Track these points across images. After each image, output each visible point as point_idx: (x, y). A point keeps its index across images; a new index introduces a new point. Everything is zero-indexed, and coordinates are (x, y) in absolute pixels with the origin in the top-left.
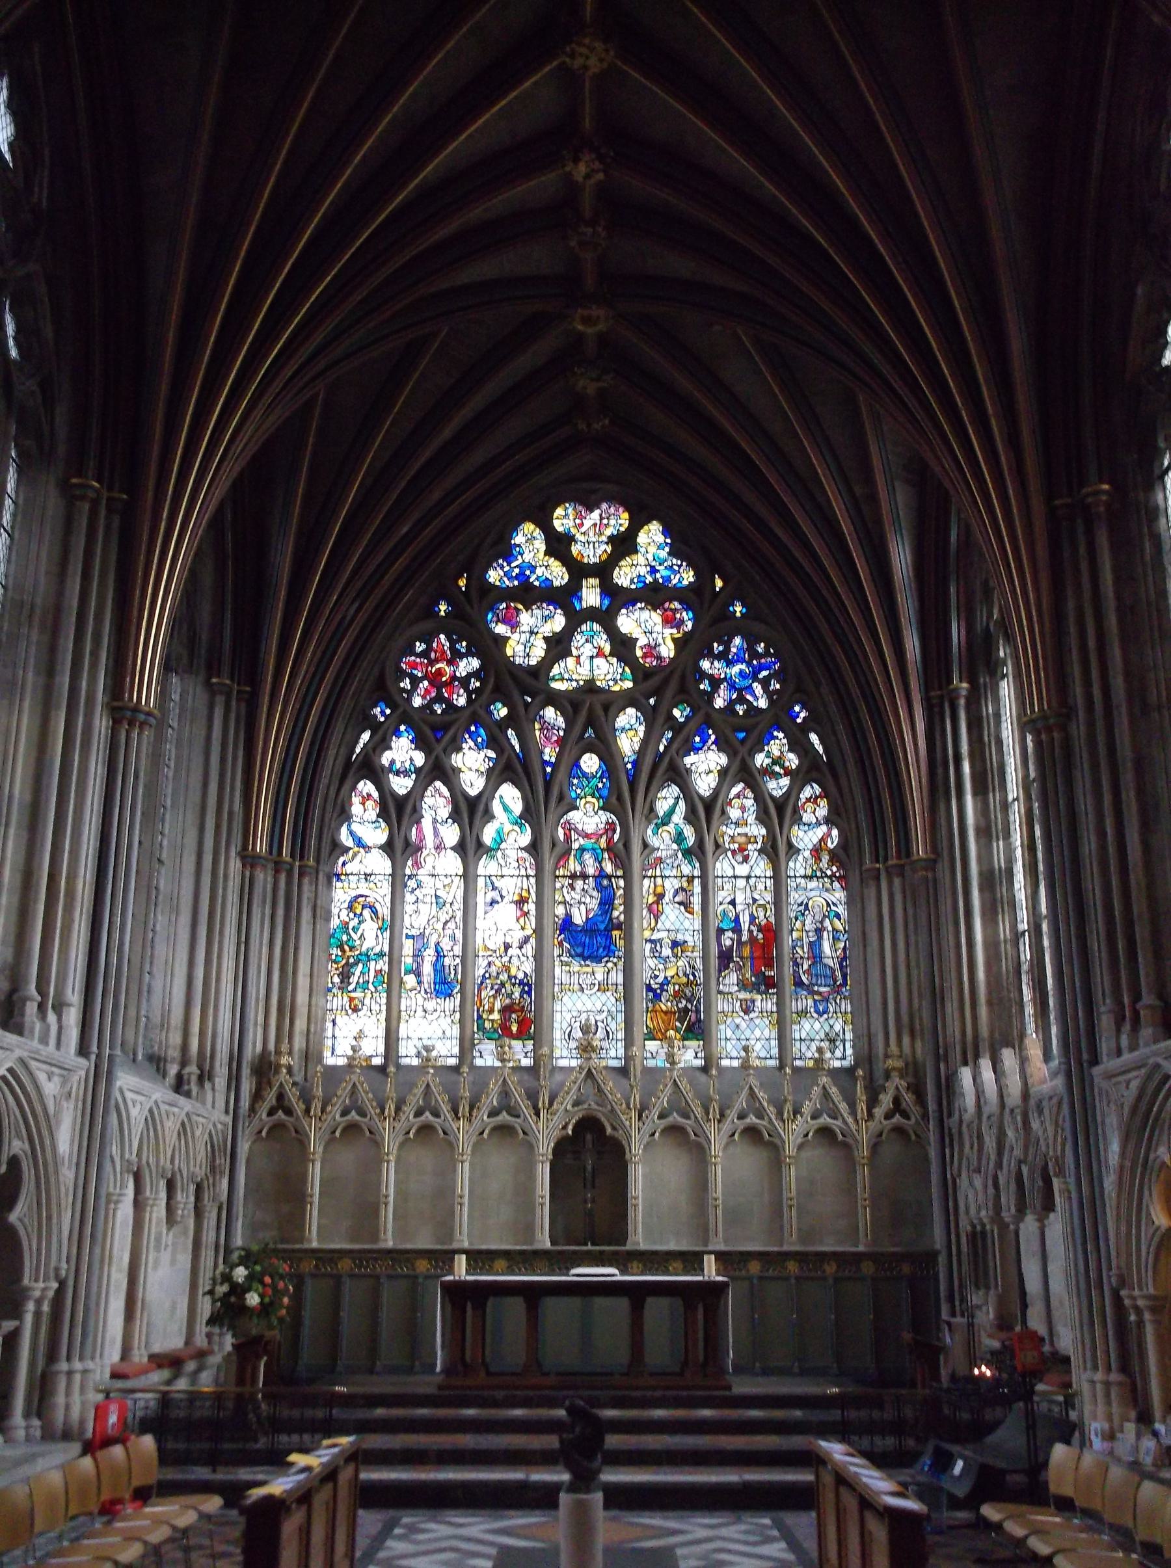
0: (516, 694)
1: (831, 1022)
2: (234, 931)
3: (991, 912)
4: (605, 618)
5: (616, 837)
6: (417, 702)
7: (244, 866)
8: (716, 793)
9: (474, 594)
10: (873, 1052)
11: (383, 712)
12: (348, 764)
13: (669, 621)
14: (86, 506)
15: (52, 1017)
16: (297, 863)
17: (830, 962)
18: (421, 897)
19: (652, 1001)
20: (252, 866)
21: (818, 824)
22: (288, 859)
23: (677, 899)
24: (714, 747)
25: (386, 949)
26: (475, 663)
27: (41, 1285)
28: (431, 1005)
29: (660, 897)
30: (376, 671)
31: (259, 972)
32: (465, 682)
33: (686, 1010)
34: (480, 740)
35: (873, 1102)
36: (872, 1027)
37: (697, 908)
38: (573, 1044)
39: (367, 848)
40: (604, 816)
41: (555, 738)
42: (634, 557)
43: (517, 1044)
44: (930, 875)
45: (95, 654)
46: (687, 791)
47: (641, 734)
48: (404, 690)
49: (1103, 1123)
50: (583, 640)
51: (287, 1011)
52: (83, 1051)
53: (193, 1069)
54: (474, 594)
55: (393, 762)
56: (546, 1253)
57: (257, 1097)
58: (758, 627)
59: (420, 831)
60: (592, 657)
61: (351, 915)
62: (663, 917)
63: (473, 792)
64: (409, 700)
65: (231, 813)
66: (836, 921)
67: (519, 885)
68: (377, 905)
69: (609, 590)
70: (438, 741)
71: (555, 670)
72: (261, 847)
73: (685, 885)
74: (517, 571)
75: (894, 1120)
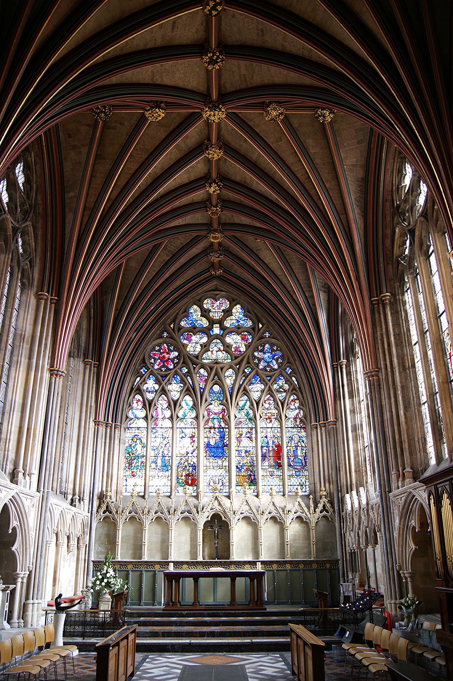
0: (191, 365)
1: (301, 479)
2: (92, 448)
3: (356, 439)
4: (221, 338)
5: (225, 414)
6: (156, 367)
7: (95, 425)
8: (260, 398)
9: (176, 330)
10: (316, 489)
11: (144, 371)
12: (132, 389)
13: (243, 339)
14: (43, 301)
15: (27, 477)
16: (114, 424)
17: (300, 458)
18: (157, 435)
19: (238, 472)
20: (98, 425)
21: (296, 409)
22: (111, 422)
23: (247, 436)
24: (259, 382)
25: (145, 454)
26: (176, 354)
27: (23, 573)
28: (161, 474)
29: (241, 435)
30: (142, 357)
31: (100, 463)
32: (173, 360)
33: (250, 475)
35: (316, 507)
36: (315, 481)
37: (254, 439)
38: (211, 488)
39: (138, 418)
40: (221, 407)
41: (204, 379)
42: (231, 317)
43: (191, 488)
44: (334, 426)
45: (45, 351)
47: (234, 378)
48: (151, 363)
49: (393, 513)
50: (214, 346)
51: (109, 476)
52: (38, 490)
53: (77, 497)
54: (176, 330)
55: (147, 388)
56: (201, 562)
57: (99, 507)
58: (274, 341)
59: (157, 412)
60: (217, 351)
61: (133, 442)
62: (242, 443)
63: (175, 399)
64: (153, 367)
65: (91, 406)
66: (302, 443)
67: (192, 431)
68: (142, 438)
69: (223, 328)
70: (163, 381)
71: (204, 356)
72: (101, 418)
73: (250, 431)
74: (191, 322)
75: (323, 513)
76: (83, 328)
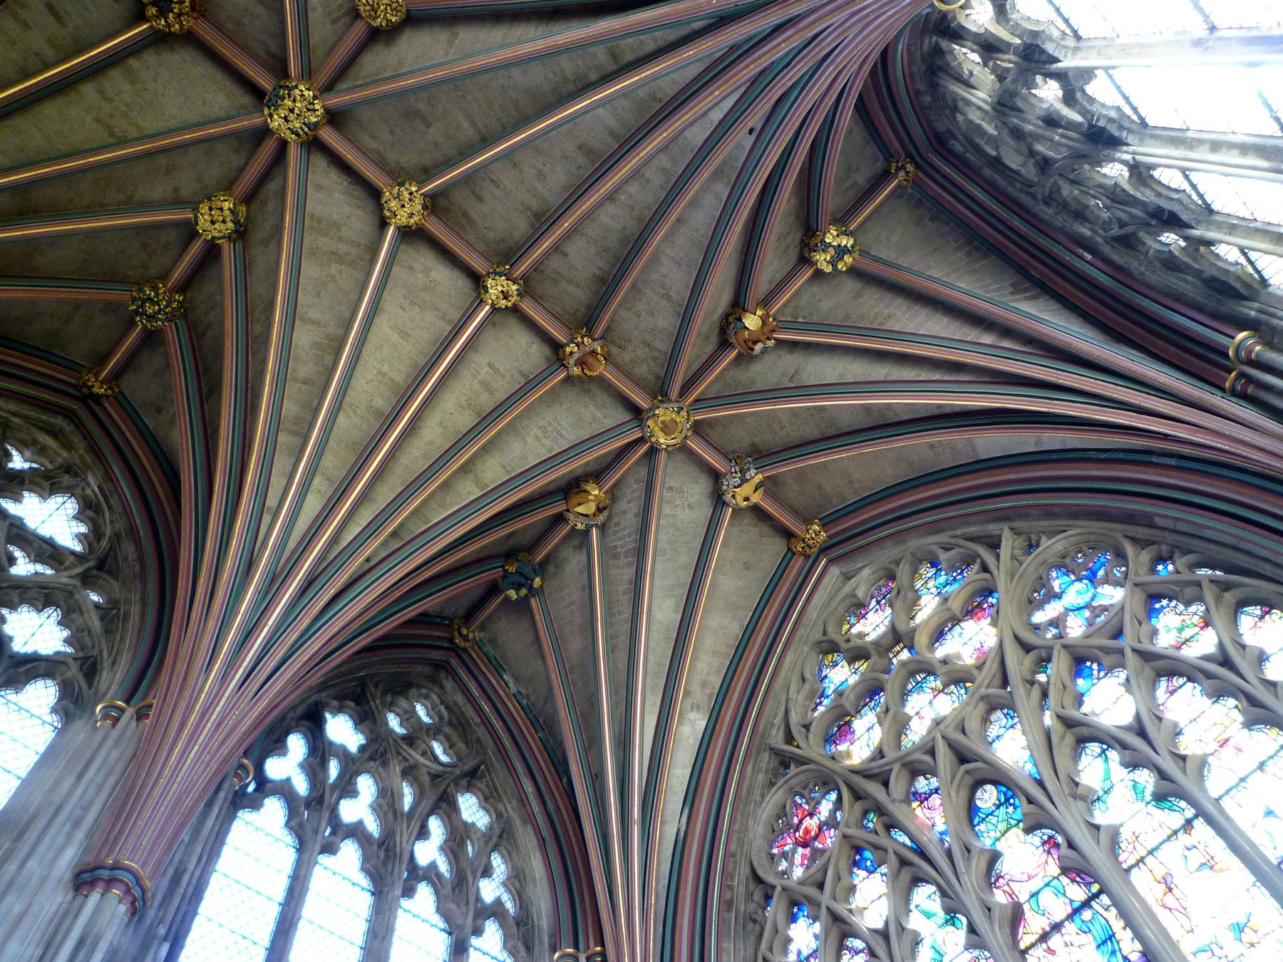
24: (1102, 673)
30: (744, 870)
34: (869, 863)
46: (1107, 739)
60: (931, 703)
76: (534, 879)
